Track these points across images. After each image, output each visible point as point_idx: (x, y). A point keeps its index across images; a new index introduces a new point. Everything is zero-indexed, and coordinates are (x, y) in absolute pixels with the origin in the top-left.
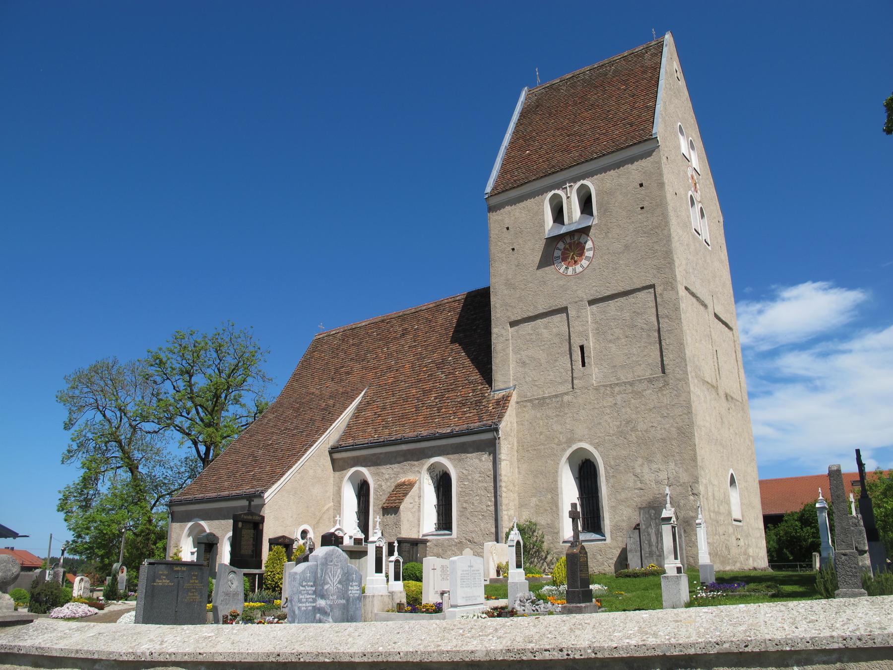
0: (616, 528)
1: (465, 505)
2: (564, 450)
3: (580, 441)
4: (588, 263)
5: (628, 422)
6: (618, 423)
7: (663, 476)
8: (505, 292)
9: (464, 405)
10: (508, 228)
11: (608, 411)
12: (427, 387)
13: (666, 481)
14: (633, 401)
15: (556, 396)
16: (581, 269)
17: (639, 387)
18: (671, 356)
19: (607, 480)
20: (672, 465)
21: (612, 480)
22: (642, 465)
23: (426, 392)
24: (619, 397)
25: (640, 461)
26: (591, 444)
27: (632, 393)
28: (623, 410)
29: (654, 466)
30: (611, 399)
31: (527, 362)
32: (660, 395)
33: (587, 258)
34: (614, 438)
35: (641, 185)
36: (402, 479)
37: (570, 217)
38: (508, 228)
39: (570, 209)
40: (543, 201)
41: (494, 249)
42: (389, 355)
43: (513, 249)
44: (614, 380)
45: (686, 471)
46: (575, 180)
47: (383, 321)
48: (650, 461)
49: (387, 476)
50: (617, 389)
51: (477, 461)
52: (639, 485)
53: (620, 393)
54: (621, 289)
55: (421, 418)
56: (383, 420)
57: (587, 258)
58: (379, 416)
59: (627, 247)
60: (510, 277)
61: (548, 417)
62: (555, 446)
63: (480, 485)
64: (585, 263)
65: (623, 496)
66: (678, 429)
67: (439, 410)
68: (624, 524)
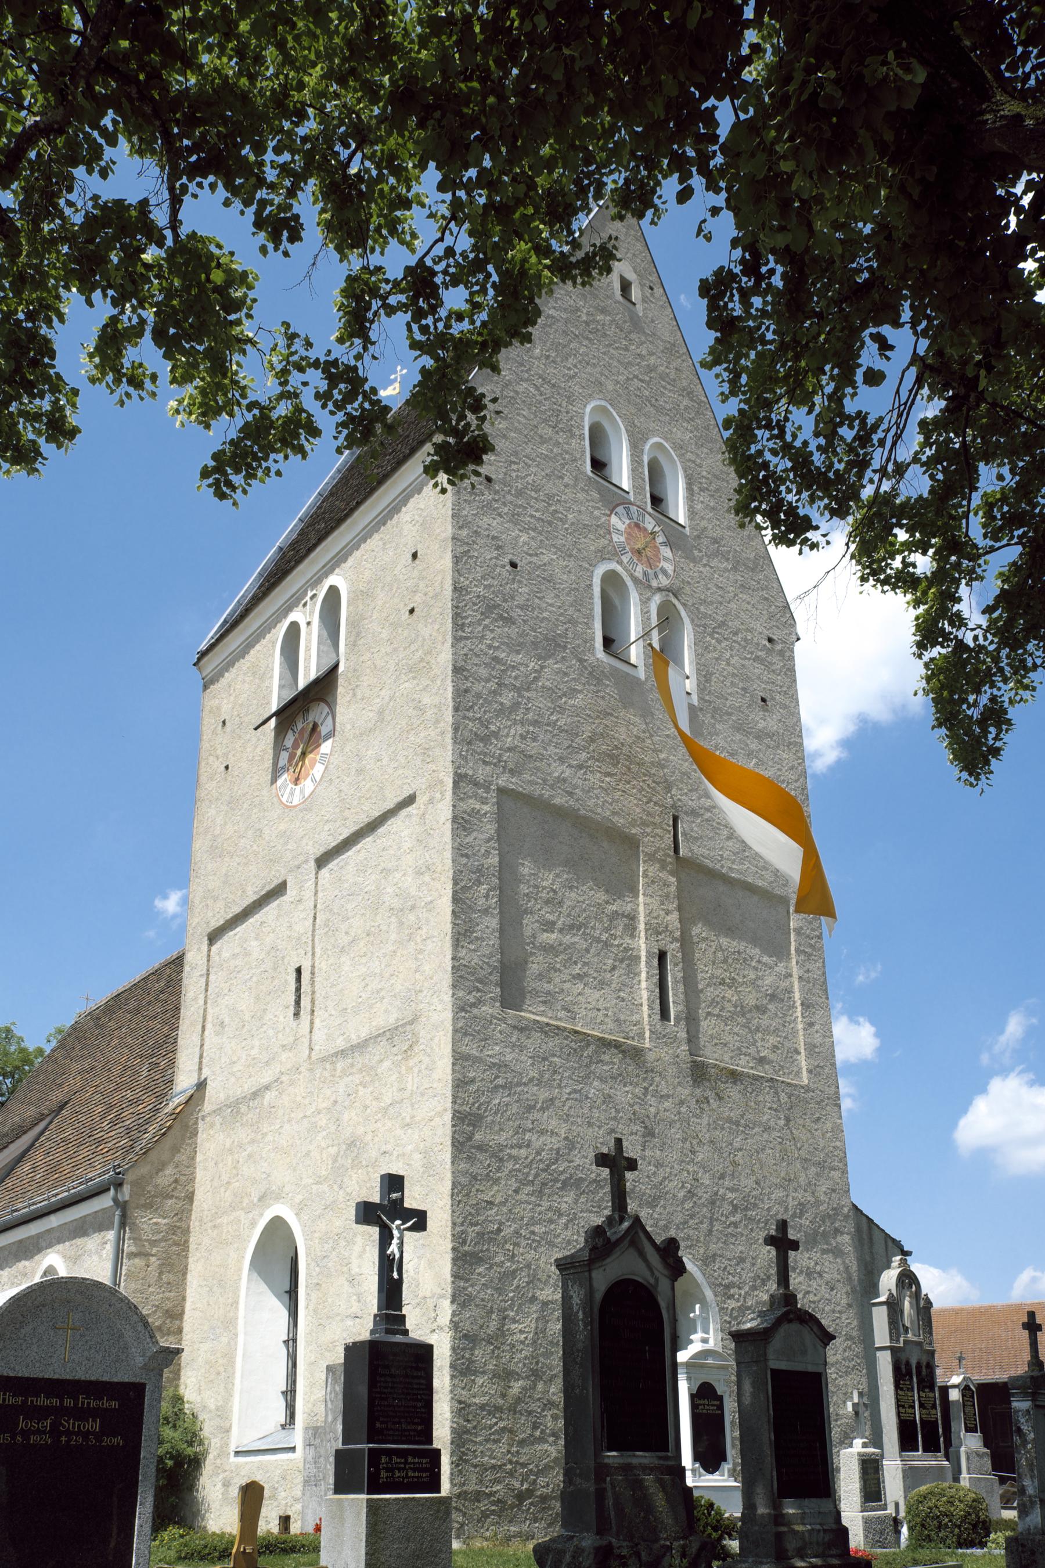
6: (333, 1151)
34: (325, 1187)
39: (308, 649)
40: (274, 643)
41: (204, 772)
43: (227, 768)
44: (340, 1043)
46: (317, 581)
54: (364, 819)
64: (318, 770)
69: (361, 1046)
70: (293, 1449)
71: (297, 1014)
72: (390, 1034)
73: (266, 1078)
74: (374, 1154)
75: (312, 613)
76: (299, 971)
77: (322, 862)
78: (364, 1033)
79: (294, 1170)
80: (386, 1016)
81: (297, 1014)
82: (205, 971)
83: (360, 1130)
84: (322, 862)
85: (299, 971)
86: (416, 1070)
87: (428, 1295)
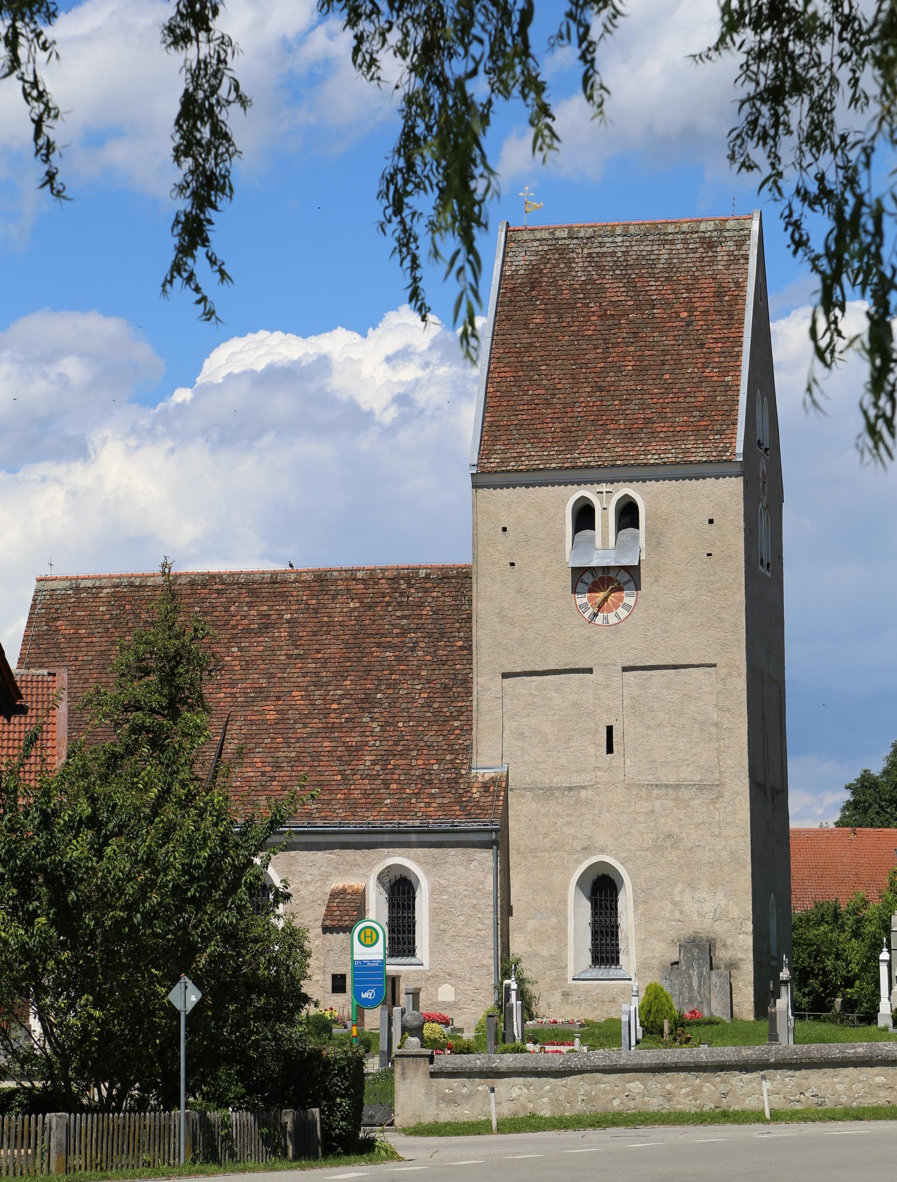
0: (644, 966)
1: (442, 927)
2: (578, 862)
3: (602, 851)
4: (627, 613)
5: (669, 836)
7: (708, 907)
8: (498, 627)
9: (430, 783)
10: (504, 529)
11: (642, 819)
12: (354, 739)
13: (711, 915)
14: (676, 811)
15: (570, 789)
16: (616, 620)
17: (685, 794)
18: (730, 762)
19: (636, 907)
20: (720, 896)
21: (641, 907)
22: (682, 892)
23: (356, 751)
24: (657, 804)
25: (680, 887)
26: (616, 858)
27: (675, 800)
28: (663, 820)
29: (699, 895)
30: (646, 804)
31: (527, 734)
32: (711, 808)
33: (626, 606)
34: (648, 854)
35: (711, 521)
36: (338, 884)
37: (605, 539)
38: (504, 529)
42: (248, 665)
44: (651, 779)
45: (737, 904)
47: (204, 586)
48: (694, 889)
49: (309, 878)
50: (655, 792)
51: (461, 869)
52: (677, 916)
53: (658, 797)
55: (357, 794)
56: (284, 788)
57: (626, 606)
58: (273, 779)
59: (683, 605)
60: (505, 605)
61: (557, 815)
62: (565, 855)
63: (466, 901)
64: (622, 612)
65: (656, 927)
66: (731, 852)
67: (386, 784)
68: (656, 962)
69: (677, 787)
70: (630, 979)
71: (610, 750)
72: (701, 787)
73: (576, 780)
74: (690, 845)
75: (608, 502)
76: (610, 730)
77: (625, 669)
78: (673, 780)
79: (616, 839)
80: (687, 774)
81: (610, 750)
82: (500, 695)
83: (676, 830)
84: (625, 669)
85: (610, 730)
86: (722, 810)
87: (736, 917)
